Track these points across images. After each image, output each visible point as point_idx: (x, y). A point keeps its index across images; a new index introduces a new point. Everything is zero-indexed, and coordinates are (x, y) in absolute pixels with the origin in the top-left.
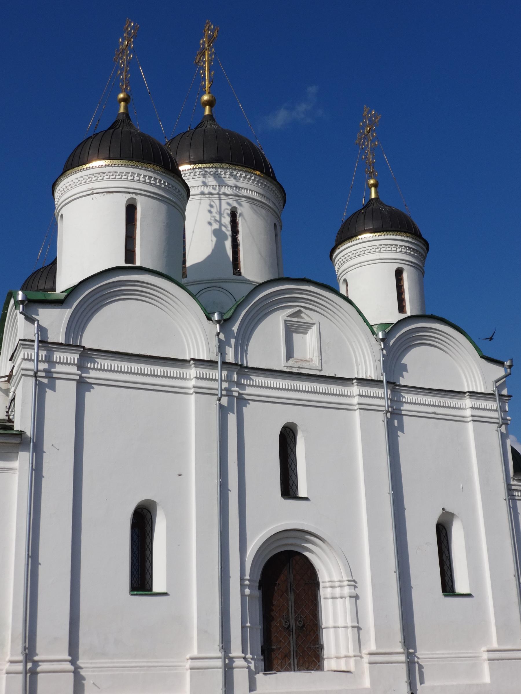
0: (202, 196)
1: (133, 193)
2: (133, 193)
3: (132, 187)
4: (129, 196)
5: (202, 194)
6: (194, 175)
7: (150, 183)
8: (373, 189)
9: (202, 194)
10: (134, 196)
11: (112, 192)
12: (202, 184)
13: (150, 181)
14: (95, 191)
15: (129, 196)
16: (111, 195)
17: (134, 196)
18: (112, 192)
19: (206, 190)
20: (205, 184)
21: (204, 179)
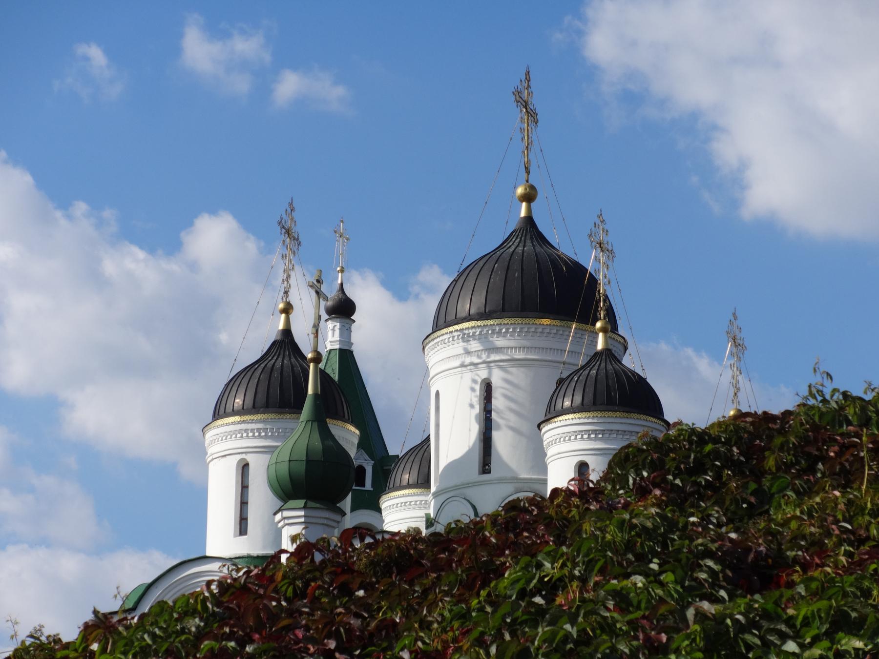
0: (463, 369)
1: (242, 453)
2: (242, 453)
3: (240, 446)
4: (239, 457)
5: (463, 365)
6: (453, 340)
7: (260, 436)
8: (601, 335)
9: (463, 365)
10: (244, 456)
11: (225, 456)
12: (462, 352)
13: (260, 433)
14: (215, 456)
15: (239, 457)
16: (224, 459)
17: (244, 456)
18: (225, 456)
19: (468, 360)
20: (468, 352)
21: (465, 344)
